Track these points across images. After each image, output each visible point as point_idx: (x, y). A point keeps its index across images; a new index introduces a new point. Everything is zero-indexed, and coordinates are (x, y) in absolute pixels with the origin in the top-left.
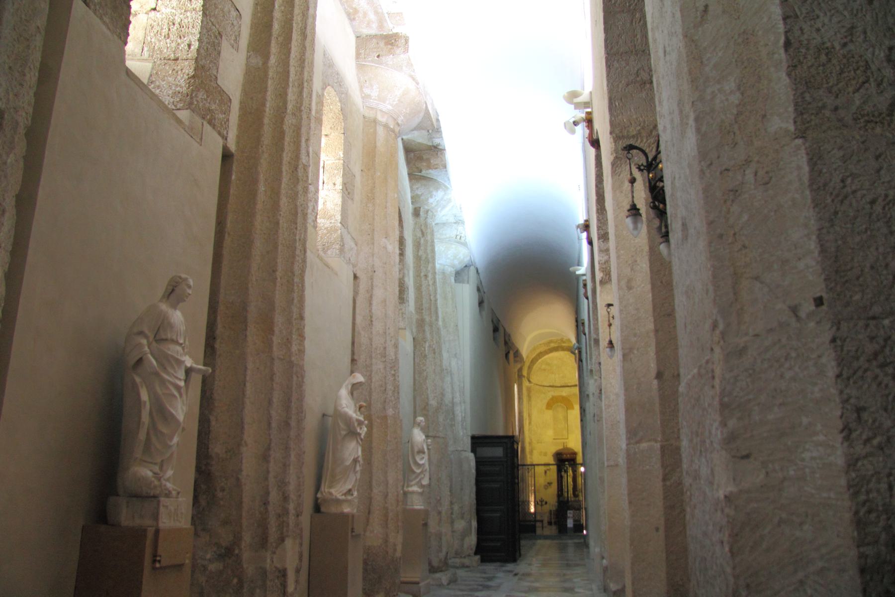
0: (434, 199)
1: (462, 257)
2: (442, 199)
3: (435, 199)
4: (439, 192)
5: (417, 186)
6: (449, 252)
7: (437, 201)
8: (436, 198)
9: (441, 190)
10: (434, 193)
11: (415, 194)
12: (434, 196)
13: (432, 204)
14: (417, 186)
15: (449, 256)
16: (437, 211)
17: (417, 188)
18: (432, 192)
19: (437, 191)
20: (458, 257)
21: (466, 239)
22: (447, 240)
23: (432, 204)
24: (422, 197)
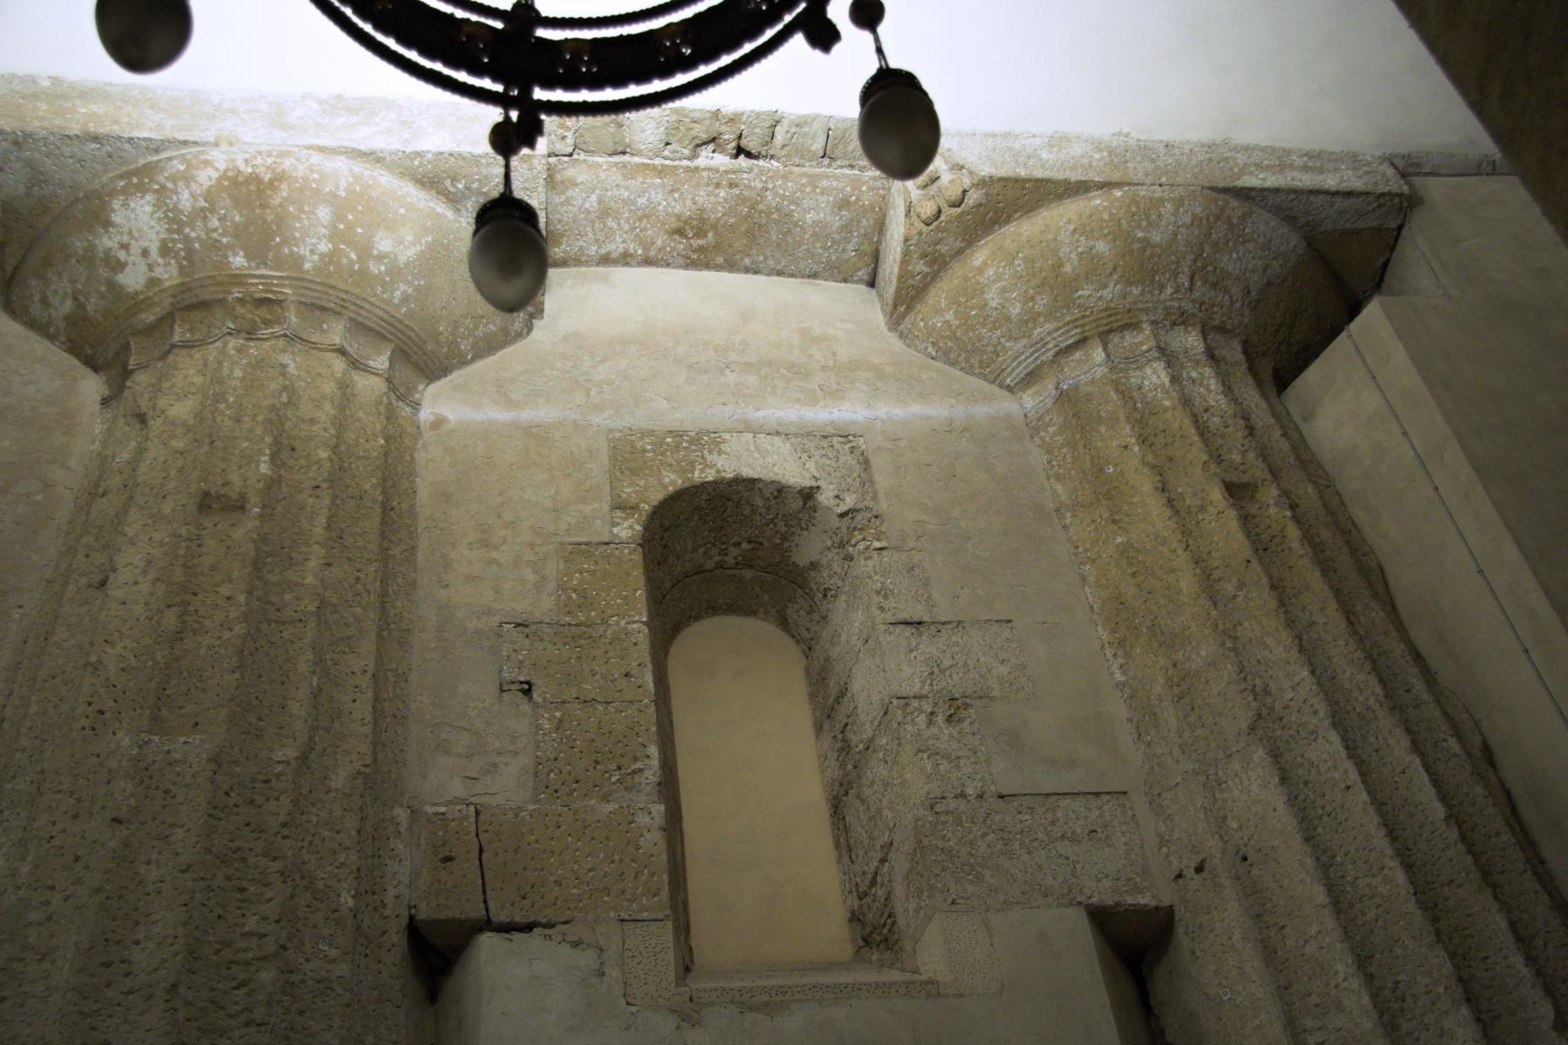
0: (134, 257)
1: (1101, 246)
2: (175, 221)
3: (145, 253)
4: (118, 218)
5: (37, 298)
6: (992, 298)
7: (165, 250)
8: (135, 248)
9: (116, 204)
10: (107, 242)
11: (62, 325)
12: (122, 255)
13: (153, 282)
14: (37, 298)
15: (1015, 310)
16: (238, 279)
17: (45, 302)
18: (91, 247)
19: (108, 224)
20: (1068, 269)
21: (971, 173)
22: (921, 267)
23: (153, 282)
24: (93, 305)
